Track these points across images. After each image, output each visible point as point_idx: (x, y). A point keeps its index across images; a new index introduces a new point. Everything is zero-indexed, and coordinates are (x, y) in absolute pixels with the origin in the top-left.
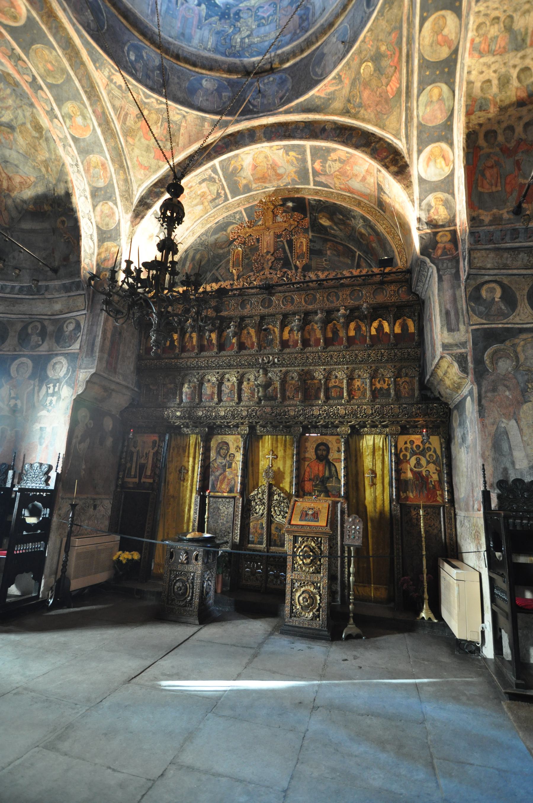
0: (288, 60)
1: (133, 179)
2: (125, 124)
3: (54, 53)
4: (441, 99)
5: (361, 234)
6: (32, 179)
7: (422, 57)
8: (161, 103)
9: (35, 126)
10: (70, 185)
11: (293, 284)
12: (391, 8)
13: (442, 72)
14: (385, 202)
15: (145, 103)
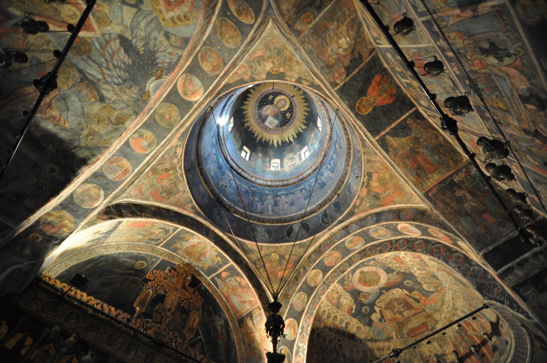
0: (237, 214)
1: (128, 190)
2: (158, 165)
3: (179, 119)
4: (303, 300)
5: (215, 329)
6: (67, 125)
7: (306, 279)
8: (182, 177)
9: (120, 118)
10: (94, 160)
11: (178, 352)
12: (299, 248)
13: (308, 291)
14: (247, 324)
15: (176, 169)
